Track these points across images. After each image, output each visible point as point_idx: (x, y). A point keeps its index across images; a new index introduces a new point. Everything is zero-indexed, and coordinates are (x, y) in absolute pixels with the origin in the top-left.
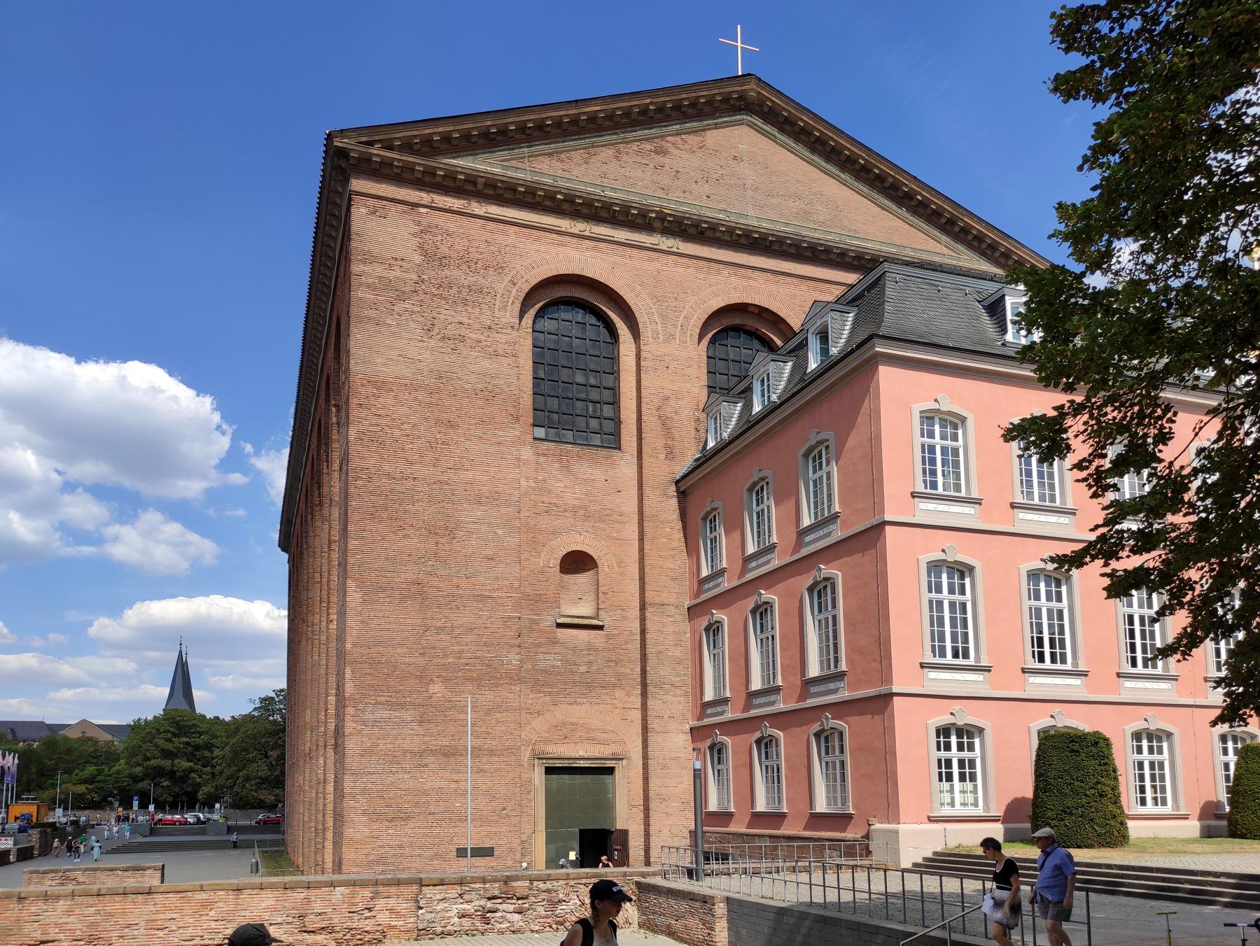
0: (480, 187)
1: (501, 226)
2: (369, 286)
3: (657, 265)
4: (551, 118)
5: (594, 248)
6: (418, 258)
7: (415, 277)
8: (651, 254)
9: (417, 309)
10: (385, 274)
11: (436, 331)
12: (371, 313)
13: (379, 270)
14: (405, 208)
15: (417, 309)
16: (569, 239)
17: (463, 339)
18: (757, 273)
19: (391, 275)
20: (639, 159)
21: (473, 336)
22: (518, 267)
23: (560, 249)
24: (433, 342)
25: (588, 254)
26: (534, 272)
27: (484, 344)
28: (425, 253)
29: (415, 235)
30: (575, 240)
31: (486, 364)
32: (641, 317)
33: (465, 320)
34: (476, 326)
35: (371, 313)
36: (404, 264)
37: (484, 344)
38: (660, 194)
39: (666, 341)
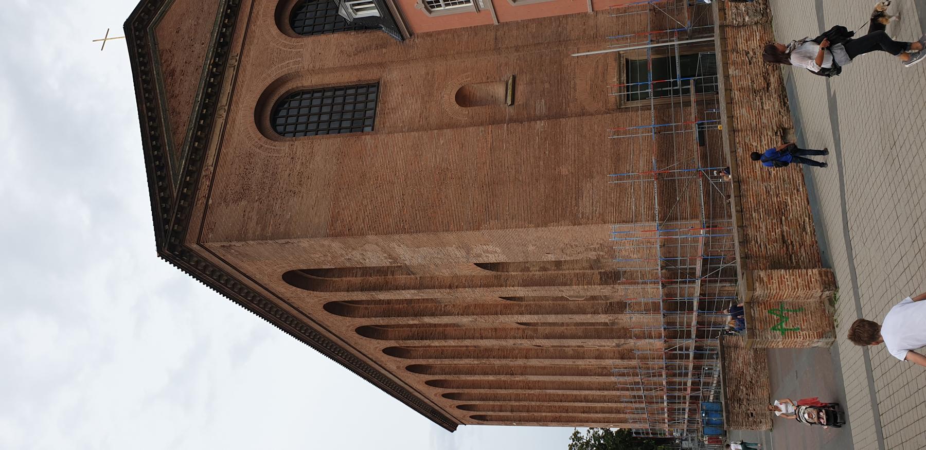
0: (194, 169)
1: (221, 156)
2: (263, 229)
3: (249, 67)
4: (150, 131)
5: (237, 103)
6: (243, 203)
7: (256, 204)
8: (240, 71)
9: (279, 201)
10: (255, 221)
11: (295, 189)
12: (282, 227)
13: (252, 224)
14: (208, 212)
15: (279, 201)
16: (230, 118)
17: (300, 173)
18: (254, 10)
19: (255, 218)
20: (177, 85)
21: (298, 168)
22: (249, 145)
23: (237, 122)
24: (303, 190)
25: (240, 106)
26: (253, 135)
27: (304, 161)
28: (240, 199)
29: (227, 206)
30: (231, 114)
31: (318, 158)
32: (285, 71)
33: (287, 173)
34: (291, 166)
35: (282, 227)
36: (248, 210)
37: (304, 161)
38: (200, 71)
39: (301, 56)
